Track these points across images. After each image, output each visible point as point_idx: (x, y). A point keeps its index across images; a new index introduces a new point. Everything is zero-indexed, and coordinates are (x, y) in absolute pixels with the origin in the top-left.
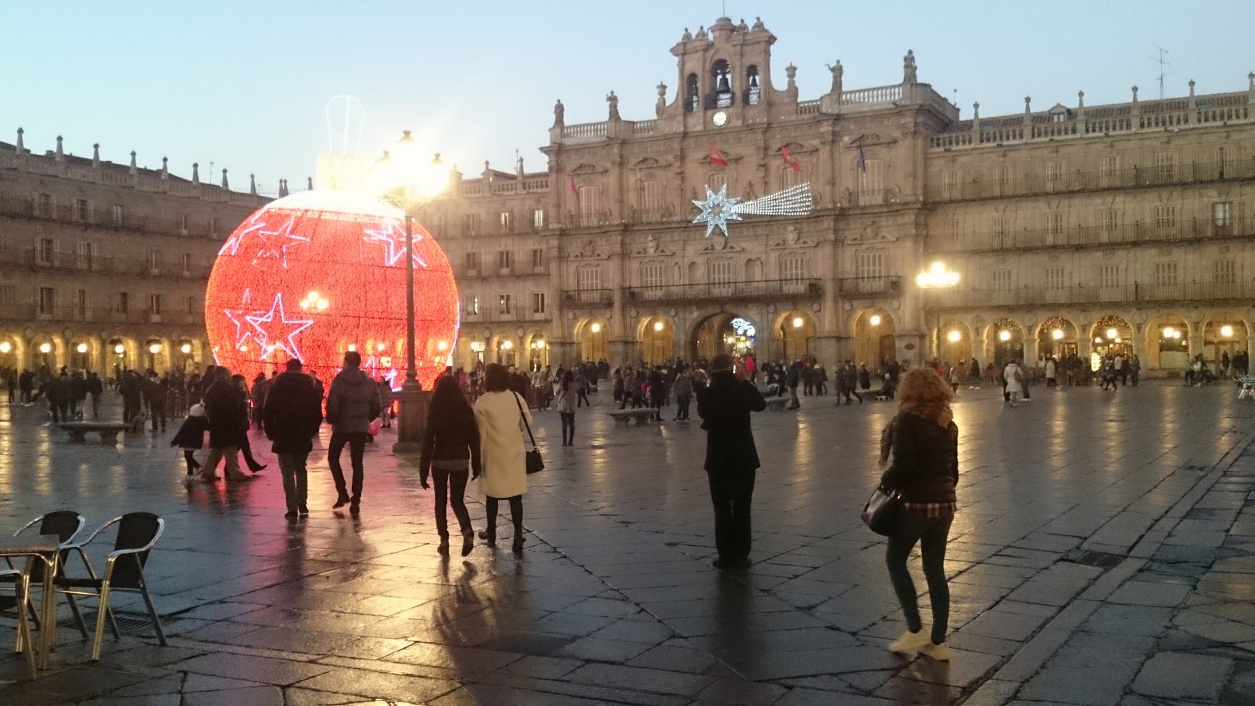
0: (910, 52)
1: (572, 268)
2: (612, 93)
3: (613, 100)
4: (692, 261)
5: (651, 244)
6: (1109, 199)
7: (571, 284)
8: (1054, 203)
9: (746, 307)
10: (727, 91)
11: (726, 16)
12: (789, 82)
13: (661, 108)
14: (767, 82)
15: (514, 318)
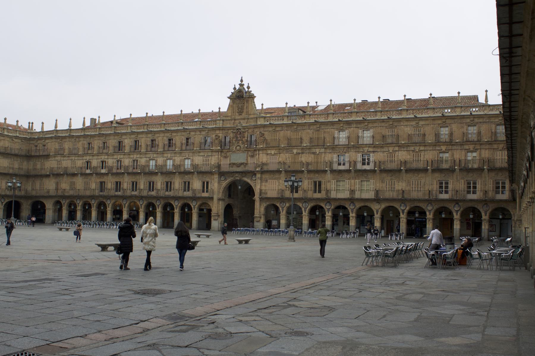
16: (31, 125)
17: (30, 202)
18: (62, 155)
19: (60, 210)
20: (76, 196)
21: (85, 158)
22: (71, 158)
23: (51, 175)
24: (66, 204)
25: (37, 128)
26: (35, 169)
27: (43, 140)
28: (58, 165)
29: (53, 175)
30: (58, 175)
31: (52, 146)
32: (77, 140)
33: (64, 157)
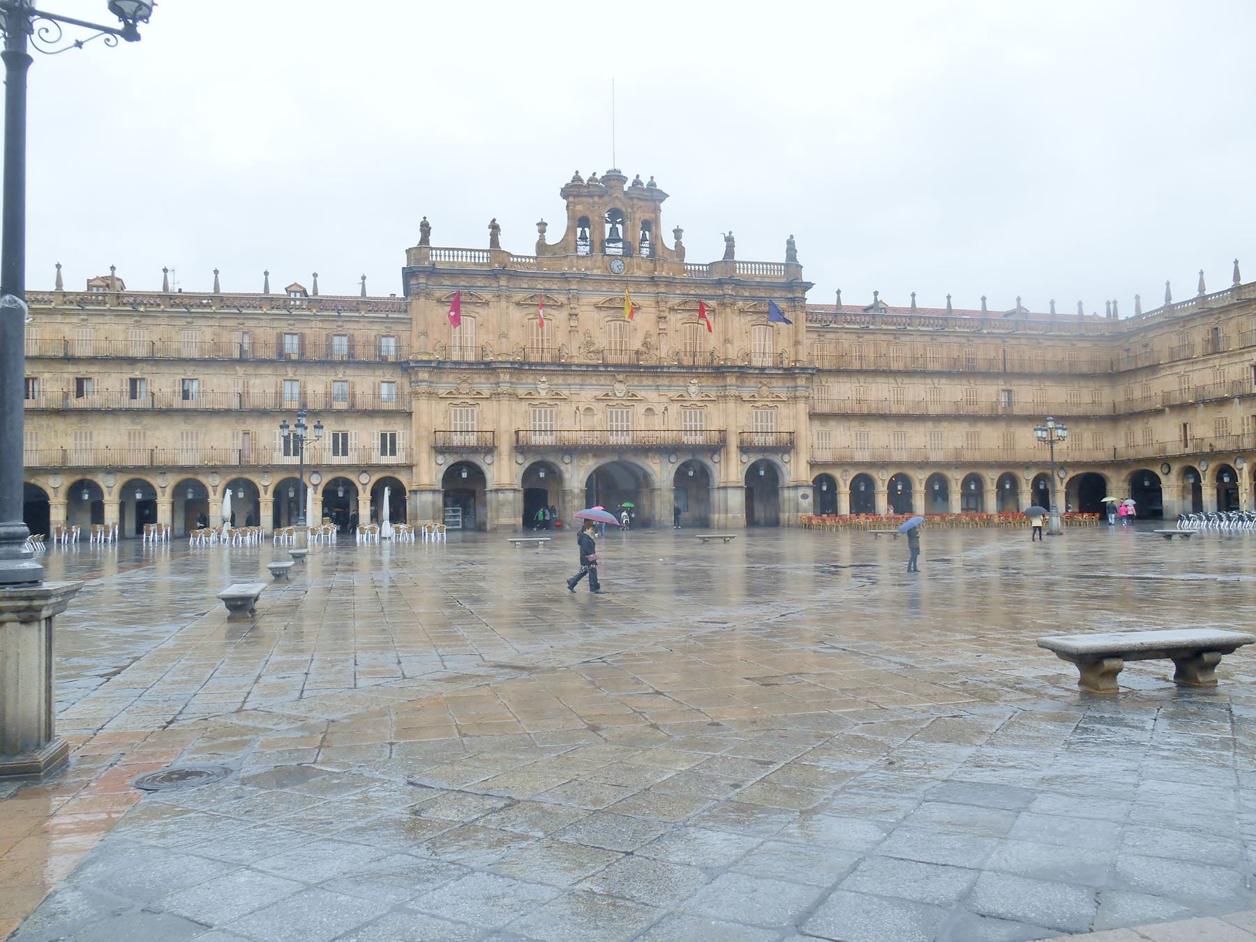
0: (792, 237)
1: (445, 404)
2: (494, 220)
3: (495, 228)
4: (586, 406)
5: (542, 386)
6: (936, 381)
7: (439, 424)
8: (899, 380)
9: (647, 457)
10: (618, 240)
11: (617, 167)
12: (676, 243)
13: (541, 246)
14: (657, 238)
15: (356, 462)
16: (1112, 306)
17: (1125, 473)
18: (1189, 359)
19: (1197, 490)
20: (1232, 452)
21: (1247, 357)
22: (1210, 363)
23: (1167, 409)
24: (1209, 473)
25: (1126, 312)
26: (1130, 400)
27: (1142, 335)
28: (1180, 383)
29: (1173, 407)
30: (1183, 407)
31: (1165, 343)
32: (1223, 317)
33: (1193, 363)
